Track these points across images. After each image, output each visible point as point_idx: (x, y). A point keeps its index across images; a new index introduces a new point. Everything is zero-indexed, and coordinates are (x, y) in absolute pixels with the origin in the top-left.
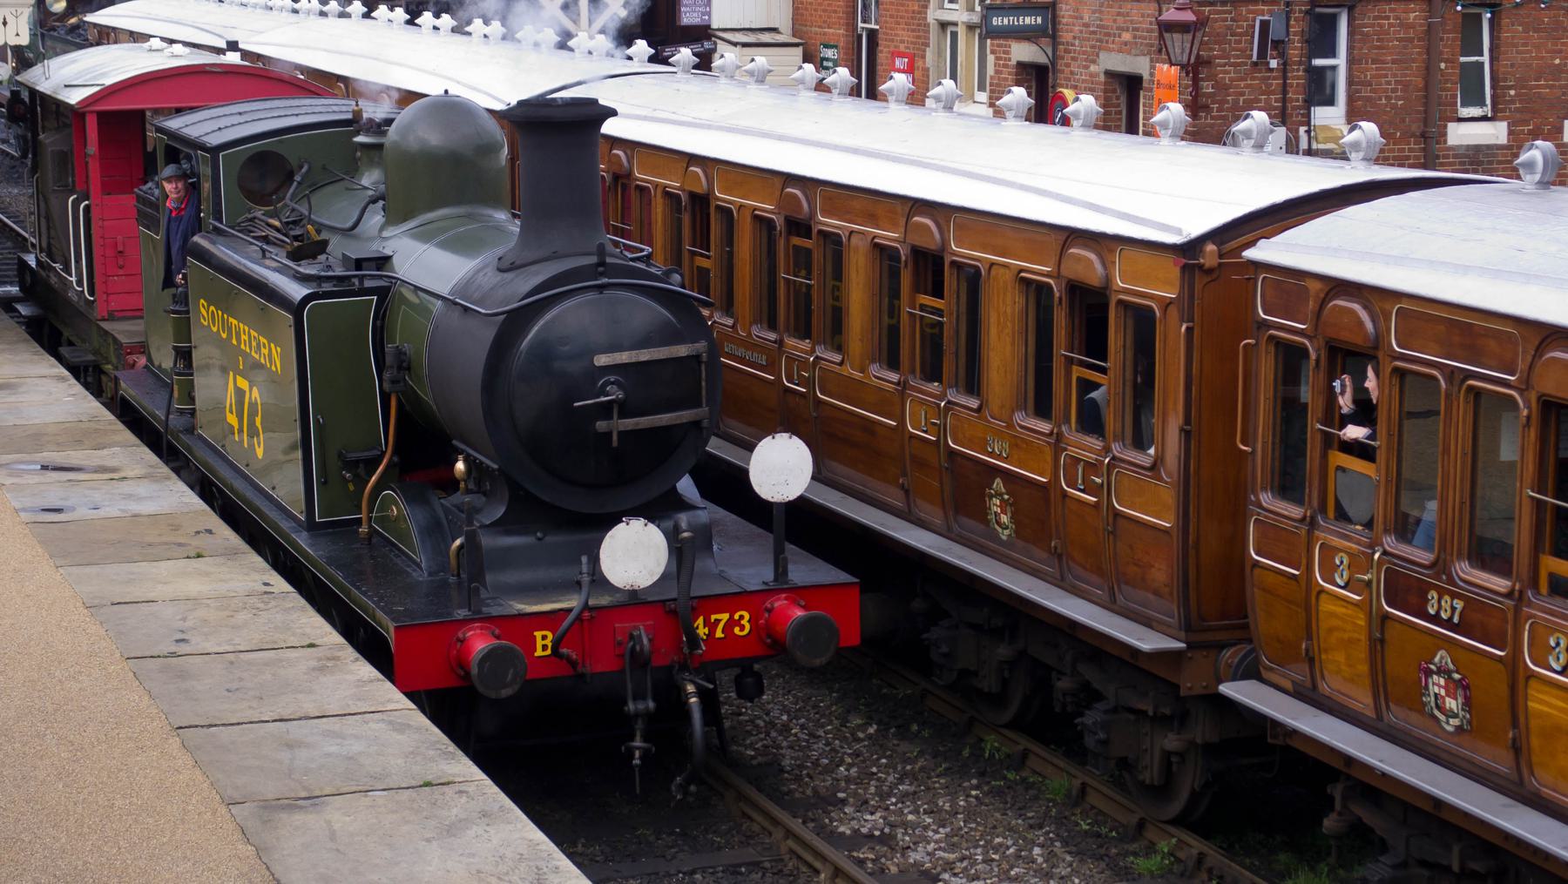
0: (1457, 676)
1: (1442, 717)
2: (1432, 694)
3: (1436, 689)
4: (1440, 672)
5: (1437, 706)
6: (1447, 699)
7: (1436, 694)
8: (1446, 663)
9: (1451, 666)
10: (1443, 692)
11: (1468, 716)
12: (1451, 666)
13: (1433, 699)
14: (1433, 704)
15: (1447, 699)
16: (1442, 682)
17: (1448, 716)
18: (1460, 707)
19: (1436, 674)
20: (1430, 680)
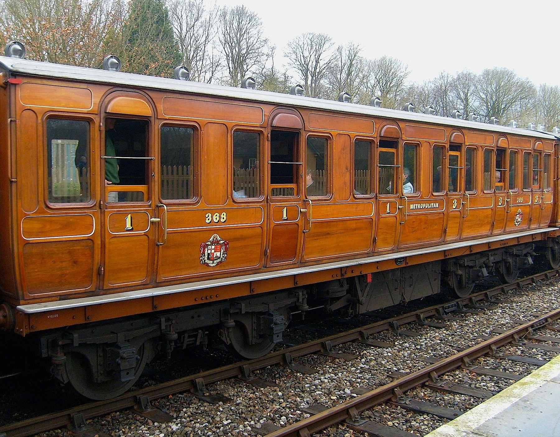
0: (222, 242)
2: (206, 254)
3: (209, 252)
7: (209, 254)
9: (219, 238)
13: (206, 256)
17: (213, 260)
18: (222, 253)
19: (210, 245)
20: (206, 249)
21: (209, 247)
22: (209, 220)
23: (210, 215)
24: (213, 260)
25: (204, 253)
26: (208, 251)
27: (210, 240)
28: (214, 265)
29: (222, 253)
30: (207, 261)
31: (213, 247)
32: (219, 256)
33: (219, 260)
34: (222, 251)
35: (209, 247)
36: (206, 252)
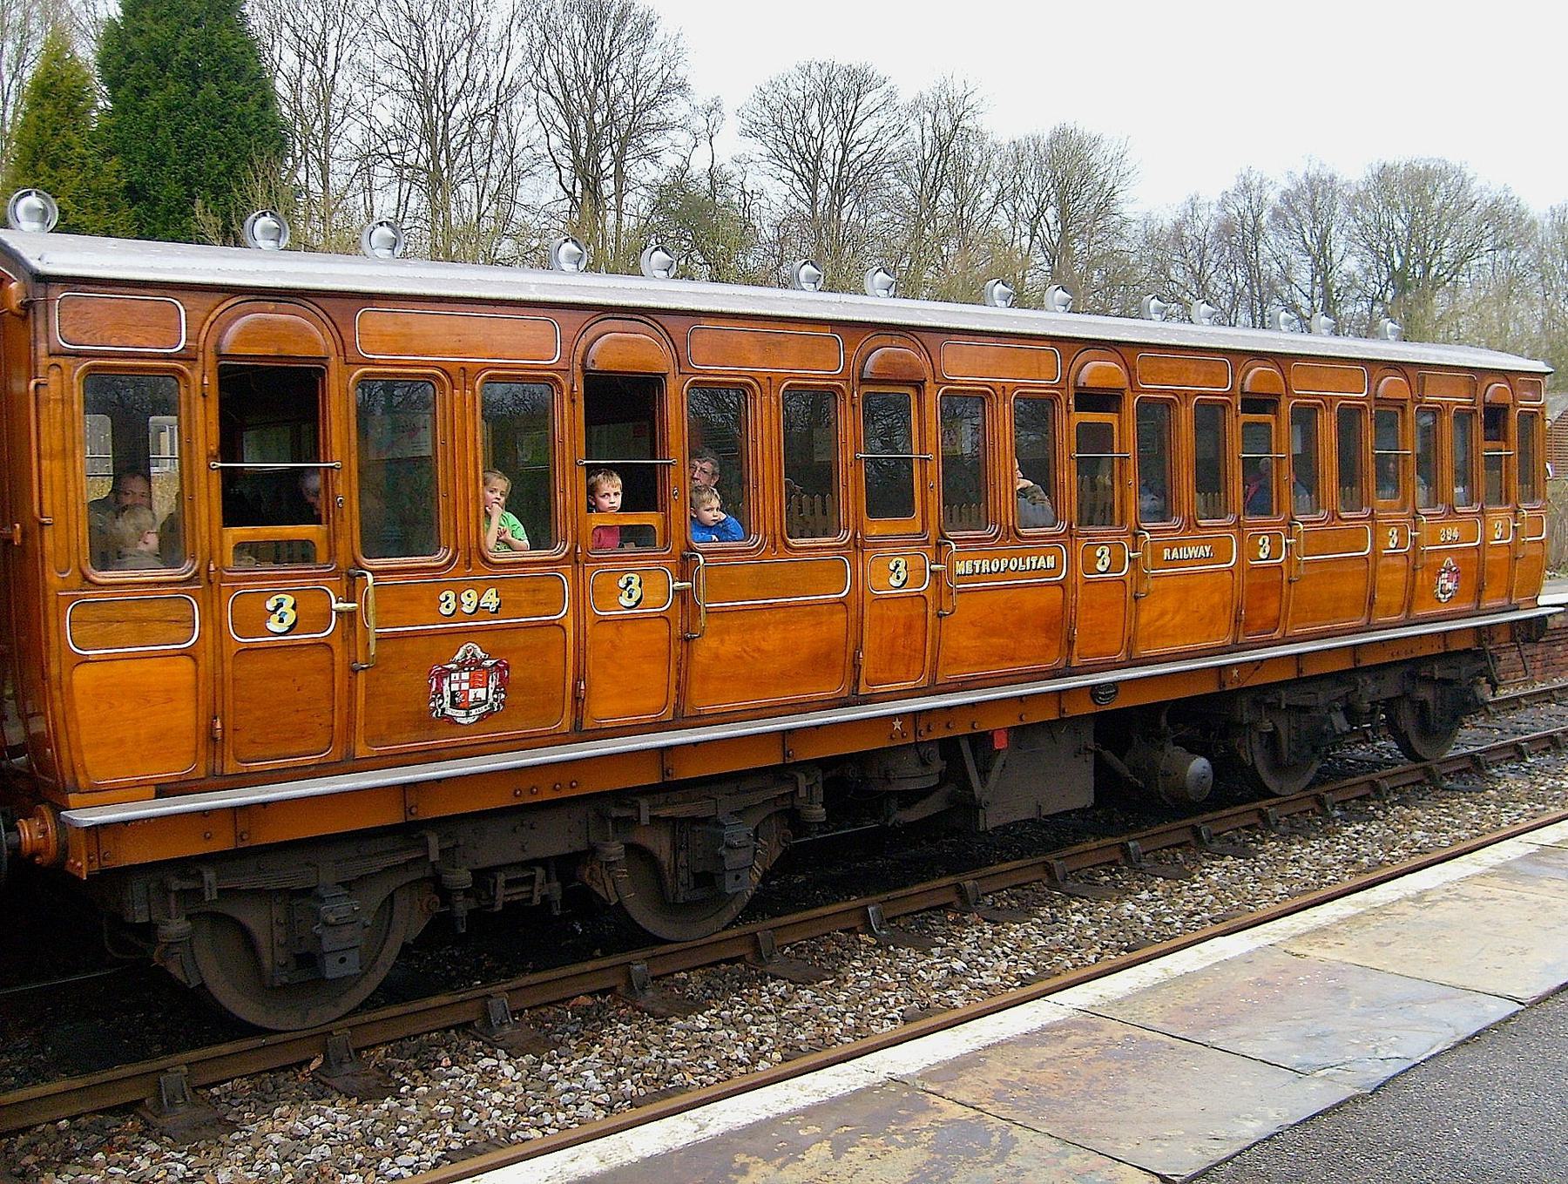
1: (463, 713)
3: (455, 687)
4: (462, 667)
5: (454, 705)
7: (453, 694)
8: (473, 655)
10: (465, 686)
11: (503, 696)
13: (447, 699)
18: (491, 691)
20: (446, 682)
21: (453, 675)
22: (448, 607)
23: (452, 595)
25: (439, 690)
26: (450, 686)
27: (457, 657)
28: (471, 720)
29: (491, 691)
30: (449, 712)
31: (465, 676)
33: (483, 710)
34: (492, 685)
35: (453, 675)
36: (446, 687)
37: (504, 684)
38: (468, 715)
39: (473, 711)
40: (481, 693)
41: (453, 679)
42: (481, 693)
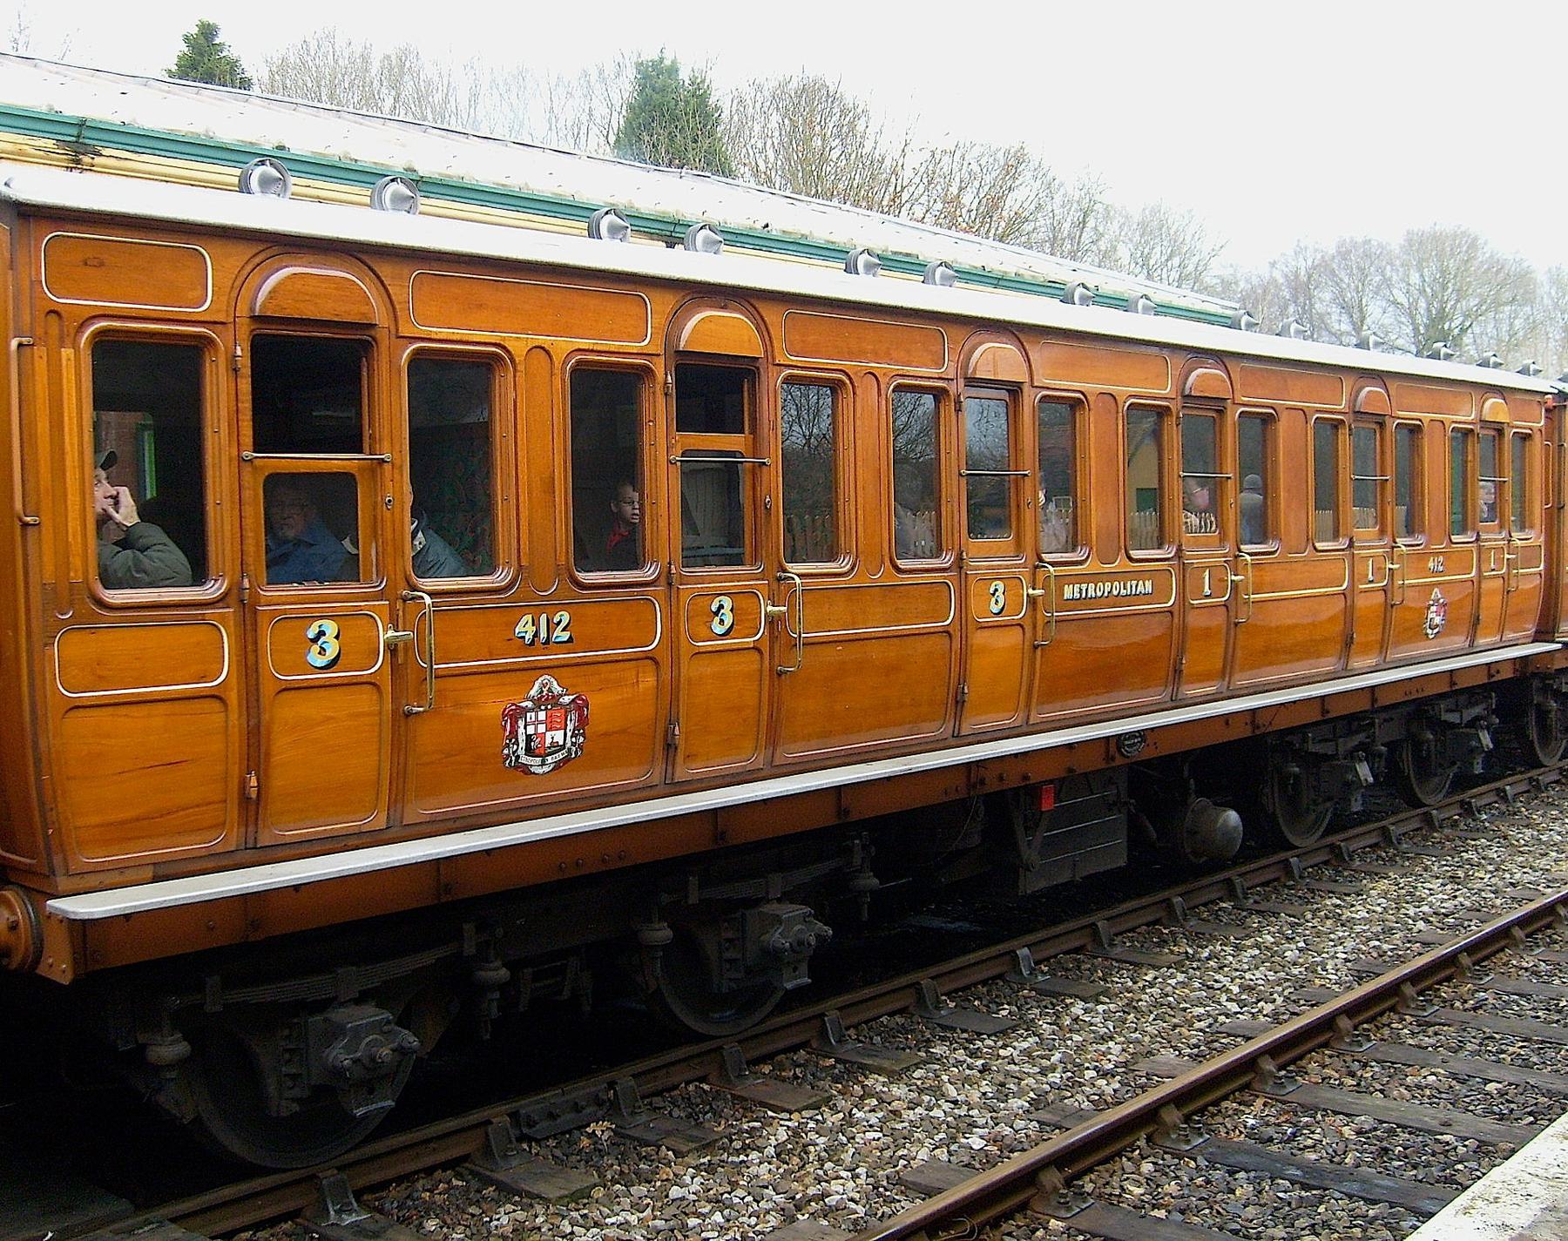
0: (567, 699)
2: (522, 739)
3: (531, 730)
6: (549, 735)
7: (529, 738)
8: (550, 690)
9: (557, 689)
10: (542, 728)
11: (582, 739)
12: (557, 689)
13: (522, 745)
14: (521, 752)
15: (549, 735)
16: (542, 715)
18: (569, 734)
20: (521, 723)
21: (528, 714)
24: (544, 756)
26: (525, 728)
27: (533, 692)
28: (546, 769)
29: (569, 734)
30: (524, 759)
31: (542, 715)
32: (561, 743)
34: (570, 726)
35: (528, 714)
36: (521, 730)
37: (583, 721)
38: (543, 764)
39: (549, 758)
40: (559, 736)
41: (528, 720)
42: (559, 736)
